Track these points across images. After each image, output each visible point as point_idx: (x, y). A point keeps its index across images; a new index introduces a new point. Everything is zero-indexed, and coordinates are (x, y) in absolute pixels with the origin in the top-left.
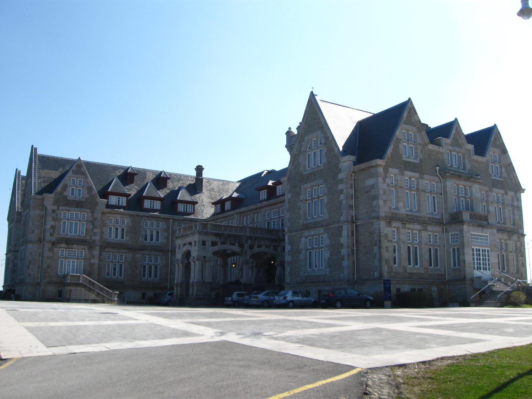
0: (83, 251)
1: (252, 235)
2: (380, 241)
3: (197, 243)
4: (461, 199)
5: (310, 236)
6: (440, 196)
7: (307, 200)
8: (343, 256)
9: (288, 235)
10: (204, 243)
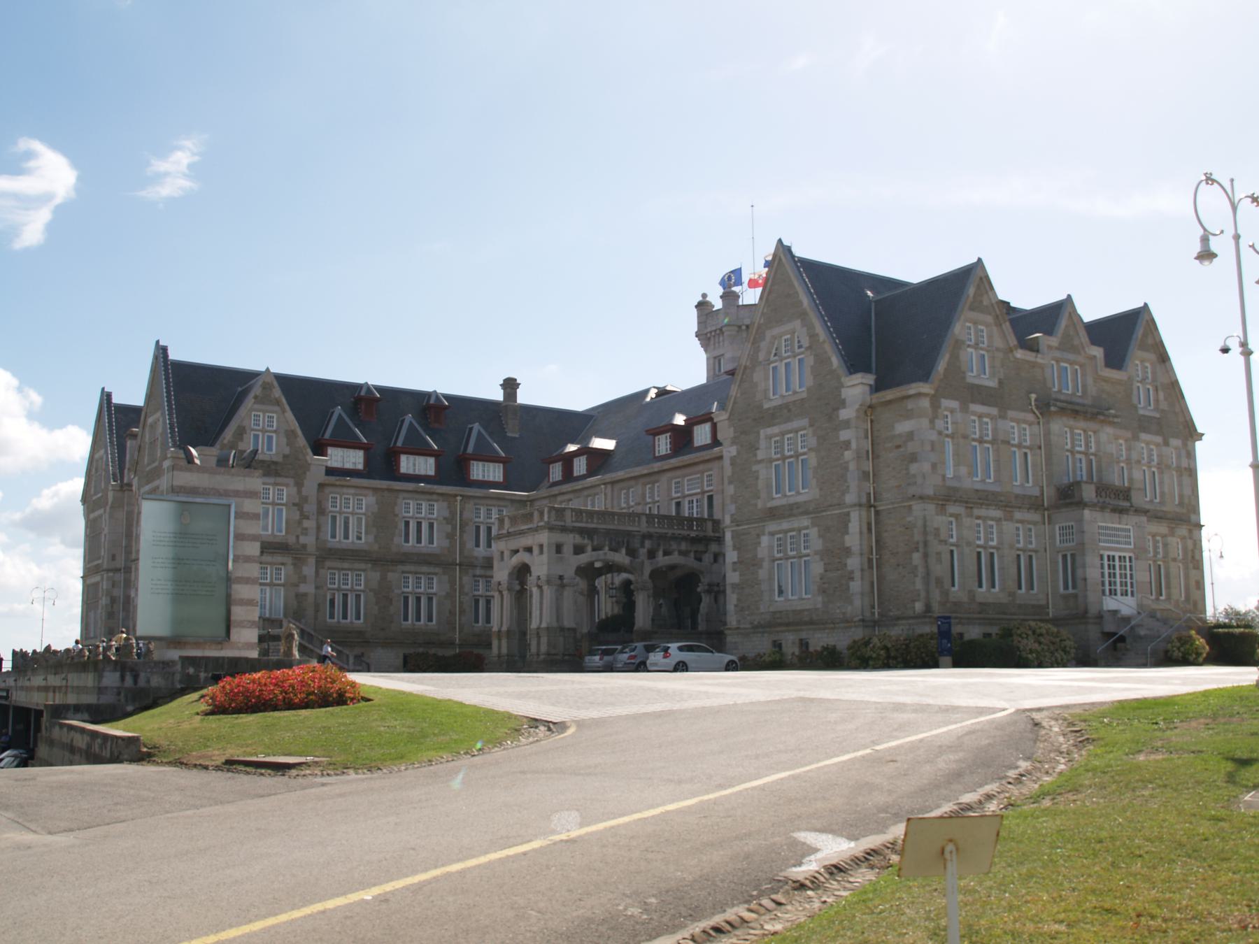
0: (283, 567)
1: (652, 530)
2: (926, 544)
3: (545, 549)
4: (1078, 456)
5: (779, 532)
6: (1038, 451)
7: (771, 461)
8: (852, 572)
9: (732, 531)
10: (559, 548)
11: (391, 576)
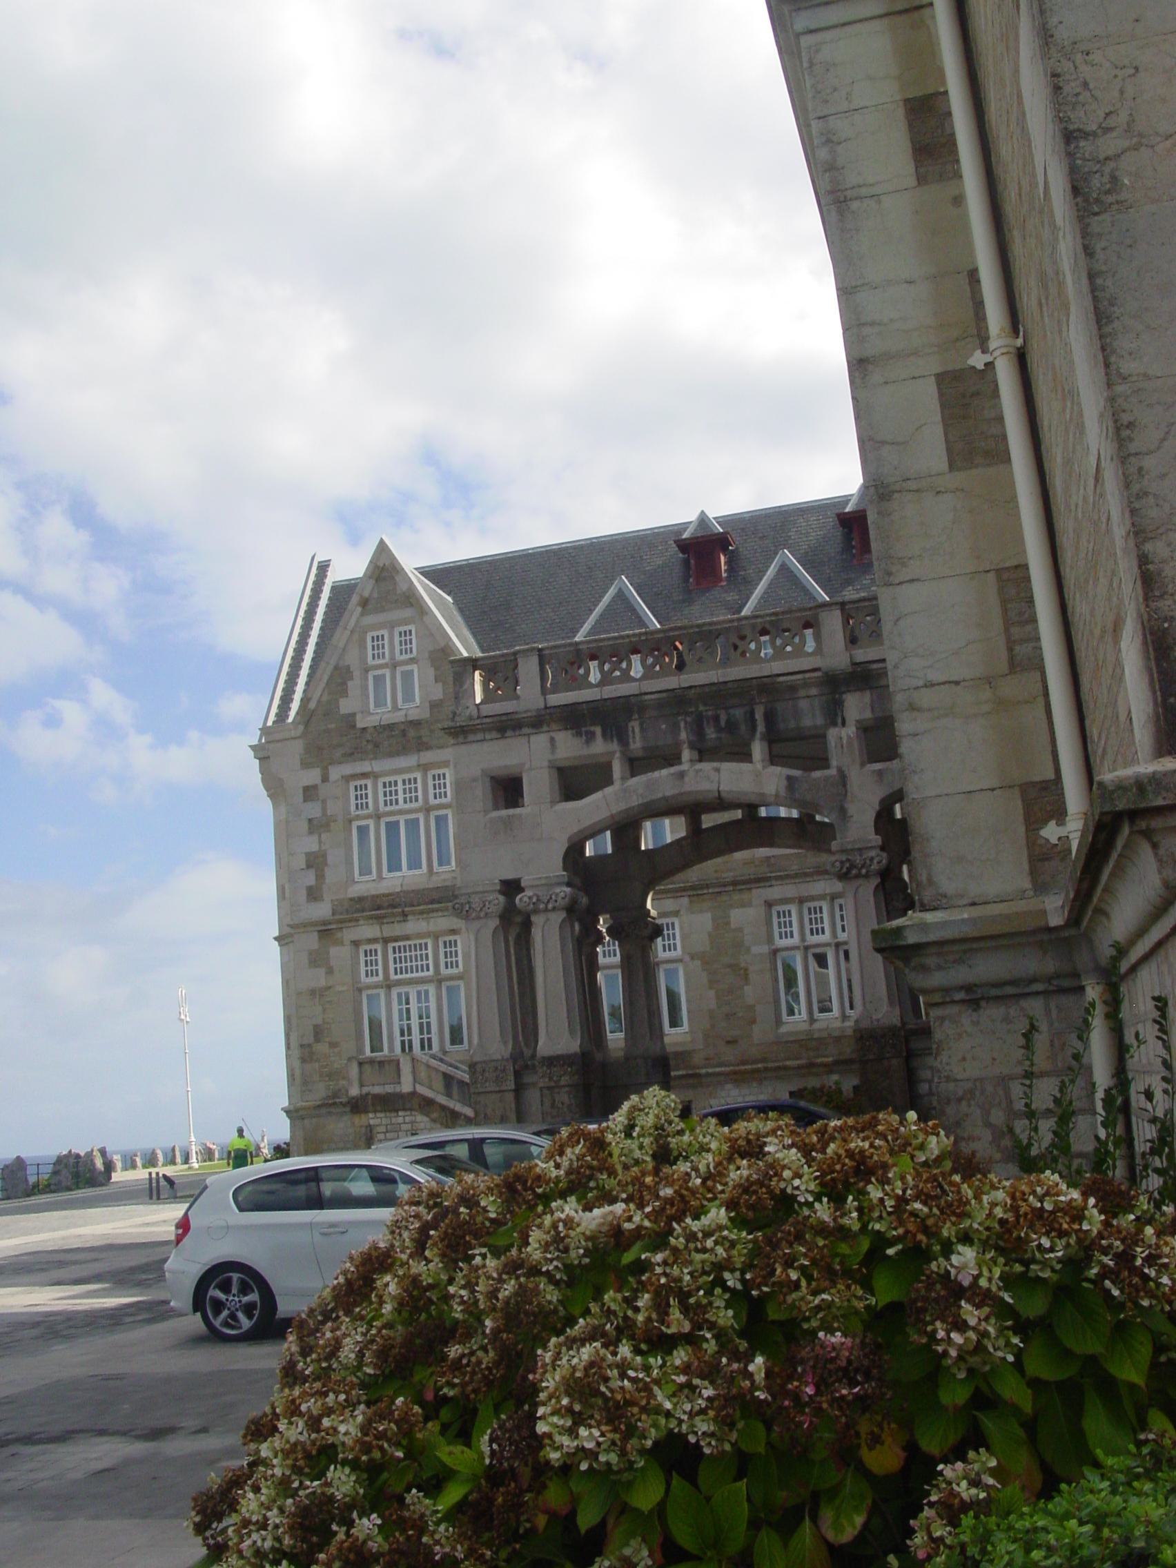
11: (738, 916)
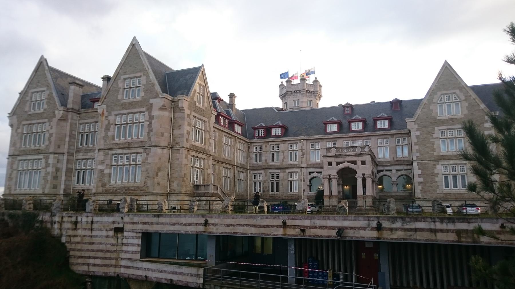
9: (418, 162)
